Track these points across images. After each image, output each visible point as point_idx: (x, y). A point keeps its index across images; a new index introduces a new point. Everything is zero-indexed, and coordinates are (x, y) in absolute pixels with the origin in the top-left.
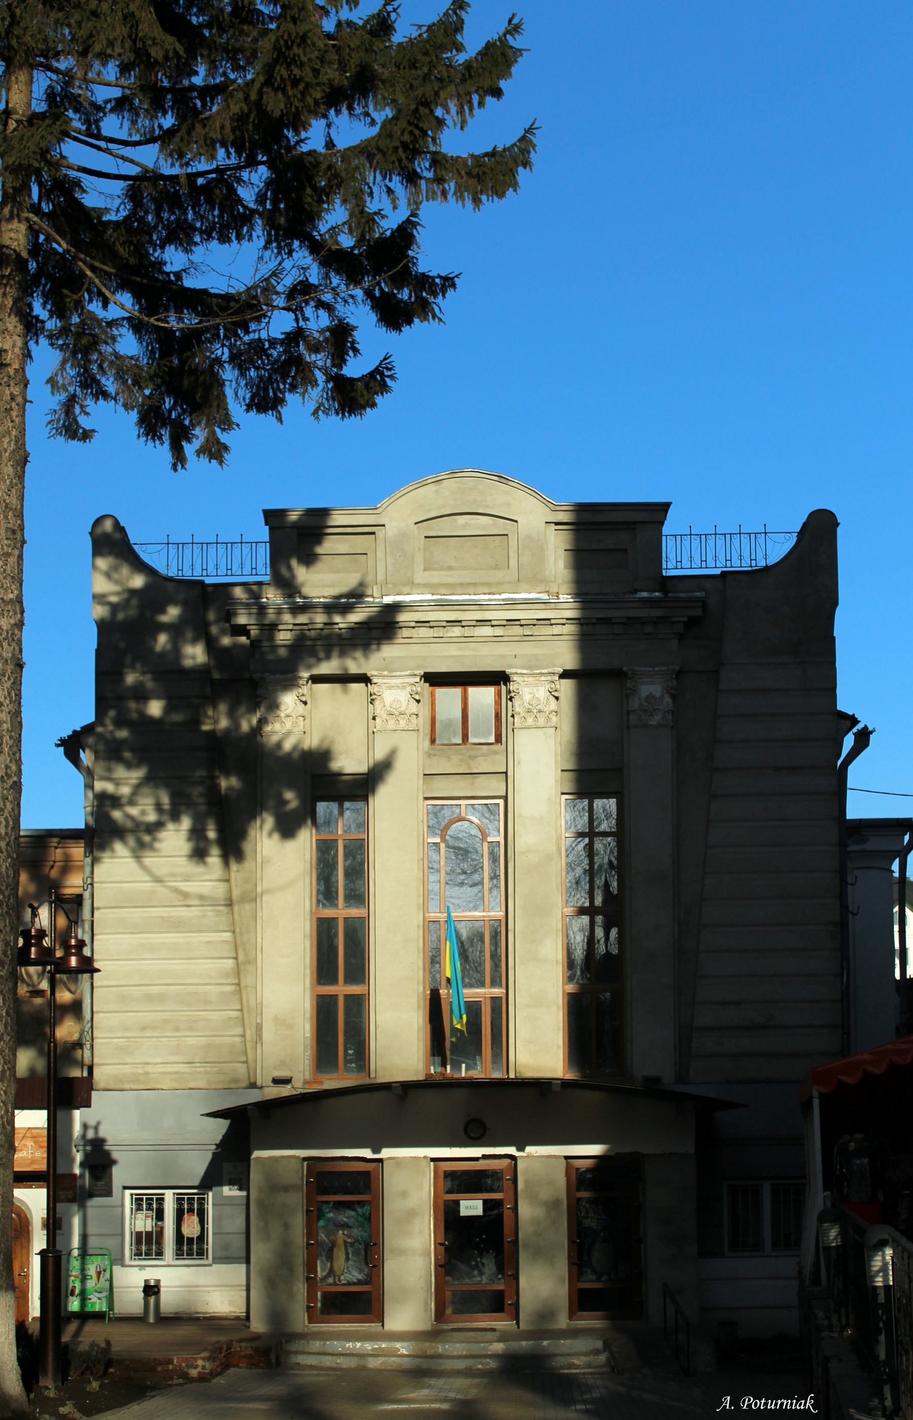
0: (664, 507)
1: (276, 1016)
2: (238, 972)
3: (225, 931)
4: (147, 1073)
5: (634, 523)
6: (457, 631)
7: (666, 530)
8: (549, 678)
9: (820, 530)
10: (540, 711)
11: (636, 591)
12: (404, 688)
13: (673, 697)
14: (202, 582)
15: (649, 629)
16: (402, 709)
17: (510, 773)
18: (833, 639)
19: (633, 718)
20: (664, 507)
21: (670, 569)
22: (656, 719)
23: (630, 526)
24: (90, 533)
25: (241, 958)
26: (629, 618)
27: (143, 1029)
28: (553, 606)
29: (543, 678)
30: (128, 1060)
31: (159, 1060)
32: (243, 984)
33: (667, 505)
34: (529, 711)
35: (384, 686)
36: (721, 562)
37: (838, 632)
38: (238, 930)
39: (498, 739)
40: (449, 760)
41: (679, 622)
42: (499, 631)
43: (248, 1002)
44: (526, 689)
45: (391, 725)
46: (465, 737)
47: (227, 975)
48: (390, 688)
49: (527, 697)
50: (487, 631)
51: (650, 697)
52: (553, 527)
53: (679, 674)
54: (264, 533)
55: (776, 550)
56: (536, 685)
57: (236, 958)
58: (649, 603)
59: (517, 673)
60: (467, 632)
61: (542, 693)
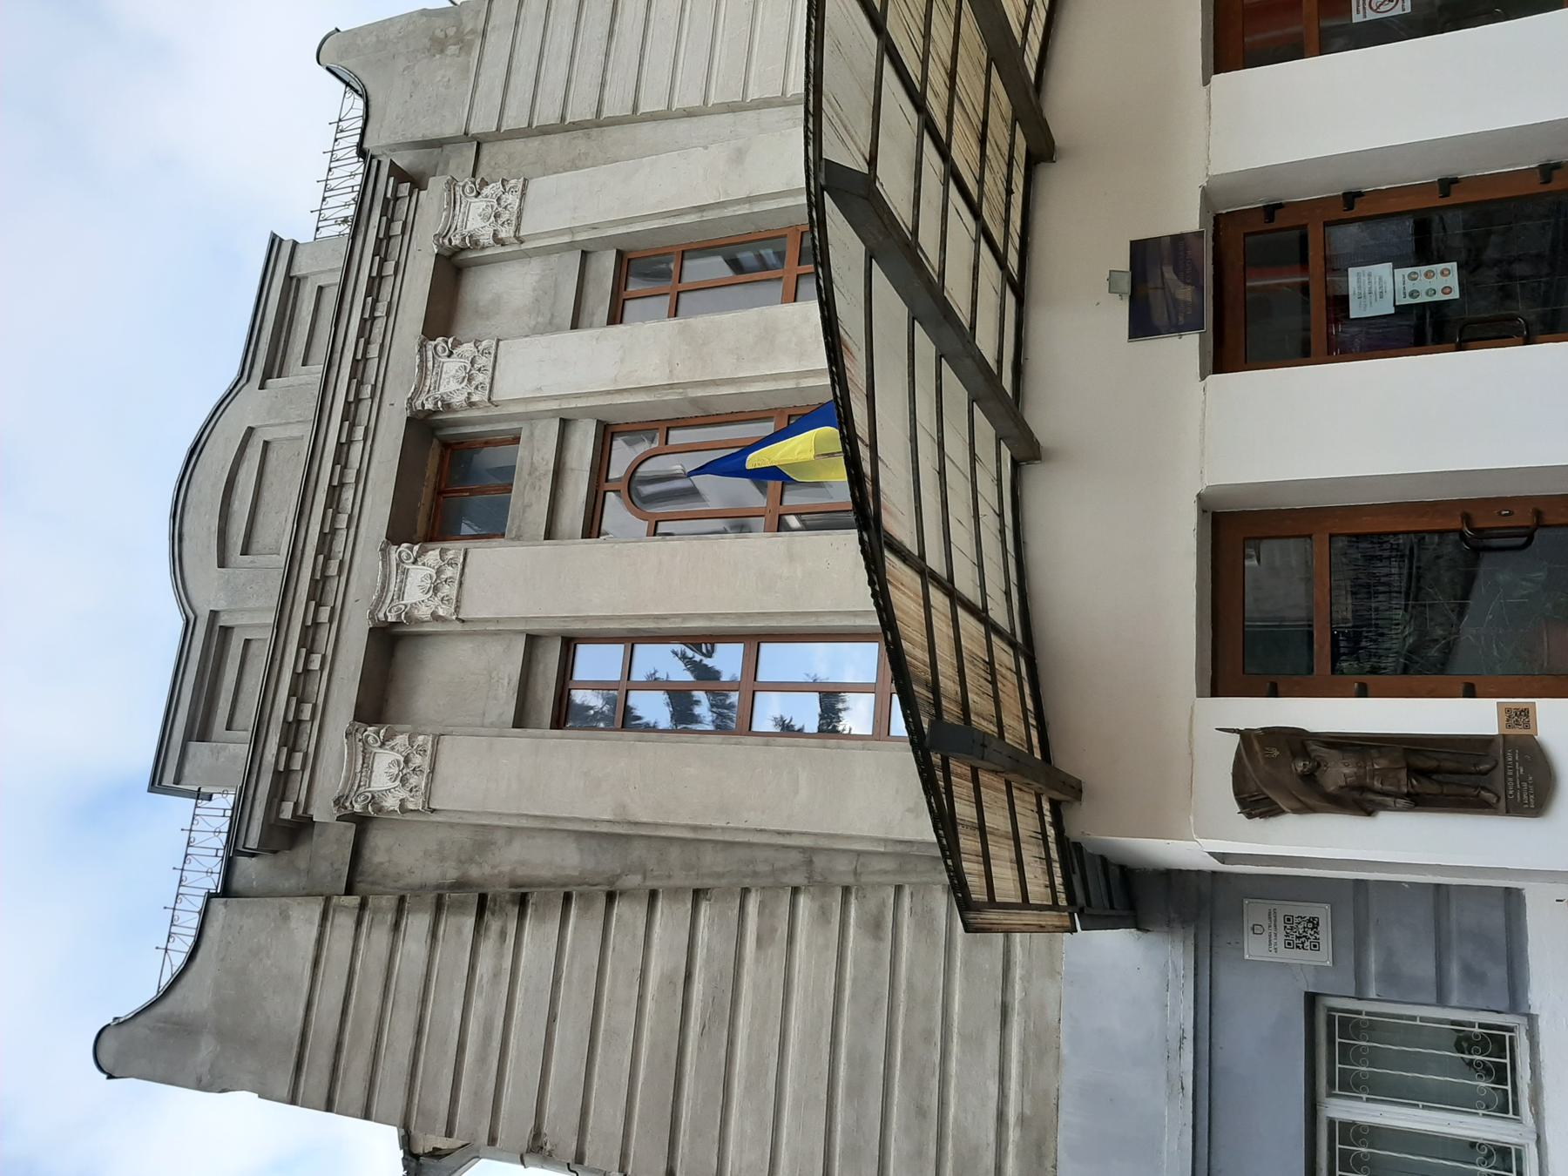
1: (909, 810)
2: (821, 886)
3: (742, 907)
4: (1022, 1120)
5: (289, 278)
6: (348, 494)
8: (430, 354)
10: (473, 363)
12: (406, 572)
14: (210, 896)
15: (397, 228)
16: (433, 572)
17: (554, 405)
19: (506, 233)
22: (512, 199)
24: (110, 1077)
25: (798, 879)
27: (921, 1112)
28: (337, 356)
29: (430, 364)
30: (989, 1160)
31: (993, 1088)
32: (849, 880)
33: (274, 238)
35: (396, 602)
38: (747, 882)
40: (530, 506)
41: (395, 190)
42: (359, 433)
43: (886, 872)
44: (442, 390)
45: (449, 590)
47: (823, 915)
48: (401, 594)
49: (454, 386)
50: (356, 450)
56: (439, 375)
57: (795, 891)
59: (411, 399)
60: (351, 477)
61: (452, 367)
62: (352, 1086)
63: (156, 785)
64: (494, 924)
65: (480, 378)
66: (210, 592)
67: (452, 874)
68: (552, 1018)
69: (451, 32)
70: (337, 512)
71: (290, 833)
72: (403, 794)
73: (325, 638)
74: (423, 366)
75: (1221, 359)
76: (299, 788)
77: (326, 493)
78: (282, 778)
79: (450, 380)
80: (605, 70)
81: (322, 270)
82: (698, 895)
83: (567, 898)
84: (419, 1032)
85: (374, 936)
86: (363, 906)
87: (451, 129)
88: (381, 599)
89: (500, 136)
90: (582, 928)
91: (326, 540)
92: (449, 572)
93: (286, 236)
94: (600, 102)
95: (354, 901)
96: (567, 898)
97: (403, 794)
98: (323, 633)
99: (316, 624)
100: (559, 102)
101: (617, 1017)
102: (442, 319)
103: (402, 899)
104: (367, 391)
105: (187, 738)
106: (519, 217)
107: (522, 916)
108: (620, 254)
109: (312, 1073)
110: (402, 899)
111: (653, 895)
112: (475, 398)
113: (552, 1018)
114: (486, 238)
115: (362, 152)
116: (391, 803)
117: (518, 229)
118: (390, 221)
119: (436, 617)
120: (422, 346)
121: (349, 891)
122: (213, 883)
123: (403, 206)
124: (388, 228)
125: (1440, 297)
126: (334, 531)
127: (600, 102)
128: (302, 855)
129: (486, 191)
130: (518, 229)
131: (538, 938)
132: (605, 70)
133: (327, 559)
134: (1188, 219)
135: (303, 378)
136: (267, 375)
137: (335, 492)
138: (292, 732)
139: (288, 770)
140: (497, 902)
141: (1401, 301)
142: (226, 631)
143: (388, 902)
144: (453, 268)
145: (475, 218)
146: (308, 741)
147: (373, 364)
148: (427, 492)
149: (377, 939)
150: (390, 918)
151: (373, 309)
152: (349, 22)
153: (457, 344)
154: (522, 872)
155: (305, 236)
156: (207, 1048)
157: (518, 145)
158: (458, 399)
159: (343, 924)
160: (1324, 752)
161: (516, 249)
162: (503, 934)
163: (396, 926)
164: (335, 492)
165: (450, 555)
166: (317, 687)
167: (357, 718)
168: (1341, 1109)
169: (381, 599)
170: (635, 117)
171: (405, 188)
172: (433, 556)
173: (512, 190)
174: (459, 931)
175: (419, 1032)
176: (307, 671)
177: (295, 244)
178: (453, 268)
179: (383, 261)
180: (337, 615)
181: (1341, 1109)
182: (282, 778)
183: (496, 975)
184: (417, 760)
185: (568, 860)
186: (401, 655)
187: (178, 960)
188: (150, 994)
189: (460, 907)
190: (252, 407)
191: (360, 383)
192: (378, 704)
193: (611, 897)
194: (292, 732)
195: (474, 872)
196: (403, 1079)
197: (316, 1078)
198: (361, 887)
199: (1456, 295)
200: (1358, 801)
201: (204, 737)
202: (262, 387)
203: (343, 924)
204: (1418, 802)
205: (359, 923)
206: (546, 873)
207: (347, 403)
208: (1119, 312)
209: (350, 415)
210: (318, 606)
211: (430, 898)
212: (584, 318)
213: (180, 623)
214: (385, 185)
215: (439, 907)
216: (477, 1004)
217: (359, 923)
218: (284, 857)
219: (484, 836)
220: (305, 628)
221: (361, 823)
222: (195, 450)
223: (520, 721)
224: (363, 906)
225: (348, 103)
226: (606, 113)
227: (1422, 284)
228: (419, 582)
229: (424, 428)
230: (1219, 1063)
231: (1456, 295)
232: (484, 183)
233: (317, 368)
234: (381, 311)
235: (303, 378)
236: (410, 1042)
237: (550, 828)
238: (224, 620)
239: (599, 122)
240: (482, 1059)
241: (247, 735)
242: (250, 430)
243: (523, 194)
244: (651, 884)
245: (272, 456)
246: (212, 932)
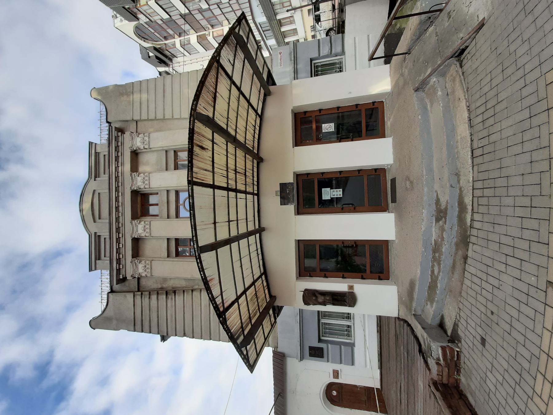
0: (91, 144)
5: (96, 153)
6: (120, 208)
14: (109, 293)
15: (120, 144)
20: (91, 144)
22: (146, 138)
26: (115, 151)
41: (117, 134)
42: (120, 194)
45: (148, 230)
46: (157, 205)
48: (137, 231)
50: (120, 198)
54: (98, 271)
60: (120, 204)
62: (146, 327)
63: (91, 270)
64: (170, 297)
65: (146, 182)
66: (94, 228)
67: (160, 286)
68: (184, 313)
69: (124, 91)
70: (119, 212)
71: (122, 280)
72: (146, 273)
73: (122, 240)
74: (132, 179)
75: (299, 212)
76: (123, 272)
77: (116, 208)
78: (119, 271)
79: (139, 183)
80: (164, 106)
81: (103, 150)
83: (184, 291)
84: (158, 317)
85: (145, 299)
86: (142, 294)
87: (129, 118)
88: (133, 233)
89: (141, 120)
90: (188, 296)
91: (117, 219)
92: (147, 226)
94: (164, 114)
95: (140, 293)
96: (184, 291)
97: (146, 273)
98: (121, 239)
99: (119, 238)
100: (154, 113)
101: (197, 313)
102: (135, 168)
103: (150, 293)
104: (120, 184)
105: (96, 260)
106: (149, 143)
107: (175, 295)
108: (175, 151)
109: (138, 325)
110: (150, 293)
113: (184, 313)
114: (142, 148)
115: (107, 122)
116: (143, 275)
117: (149, 146)
118: (118, 142)
120: (131, 175)
121: (139, 291)
122: (108, 289)
123: (120, 138)
124: (117, 144)
125: (339, 196)
126: (119, 217)
127: (164, 114)
128: (127, 283)
129: (140, 136)
130: (149, 146)
131: (179, 298)
132: (164, 106)
133: (119, 223)
134: (290, 179)
135: (104, 178)
136: (96, 177)
137: (117, 208)
138: (119, 261)
139: (120, 269)
140: (170, 292)
141: (332, 197)
142: (99, 236)
143: (147, 293)
144: (135, 154)
145: (138, 143)
146: (123, 262)
147: (120, 178)
148: (139, 206)
149: (146, 301)
150: (148, 296)
151: (118, 164)
153: (140, 174)
154: (174, 286)
155: (98, 142)
156: (114, 322)
157: (146, 123)
158: (142, 187)
159: (138, 298)
160: (319, 296)
161: (150, 150)
162: (172, 299)
163: (150, 298)
164: (117, 208)
165: (147, 222)
166: (122, 251)
167: (133, 257)
168: (323, 321)
169: (133, 233)
170: (173, 118)
171: (120, 134)
172: (143, 223)
173: (146, 136)
174: (163, 298)
175: (158, 317)
176: (119, 248)
177: (96, 144)
178: (135, 154)
179: (118, 152)
180: (124, 235)
181: (323, 321)
182: (119, 271)
183: (172, 306)
184: (147, 266)
185: (183, 284)
186: (140, 242)
187: (105, 304)
188: (100, 313)
189: (162, 294)
190: (93, 185)
191: (118, 182)
192: (136, 253)
193: (192, 291)
194: (119, 261)
195: (164, 286)
196: (157, 326)
197: (138, 326)
198: (141, 289)
199: (341, 196)
200: (324, 304)
201: (99, 259)
203: (138, 298)
204: (334, 304)
205: (142, 297)
206: (179, 286)
207: (116, 187)
208: (279, 198)
209: (117, 190)
210: (119, 234)
211: (156, 292)
212: (169, 167)
213: (88, 236)
214: (114, 133)
215: (158, 294)
216: (169, 312)
217: (142, 297)
218: (123, 284)
219: (165, 280)
220: (117, 239)
221: (139, 279)
222: (82, 195)
223: (168, 256)
224: (142, 294)
225: (102, 107)
226: (166, 117)
227: (335, 193)
228: (140, 228)
229: (135, 193)
230: (304, 316)
231: (341, 196)
232: (139, 134)
233: (107, 175)
234: (120, 165)
235: (104, 178)
236: (156, 319)
237: (178, 278)
238: (98, 234)
239: (164, 119)
240: (172, 321)
241: (108, 258)
242: (94, 191)
243: (149, 137)
244: (200, 287)
245: (101, 196)
246: (110, 300)
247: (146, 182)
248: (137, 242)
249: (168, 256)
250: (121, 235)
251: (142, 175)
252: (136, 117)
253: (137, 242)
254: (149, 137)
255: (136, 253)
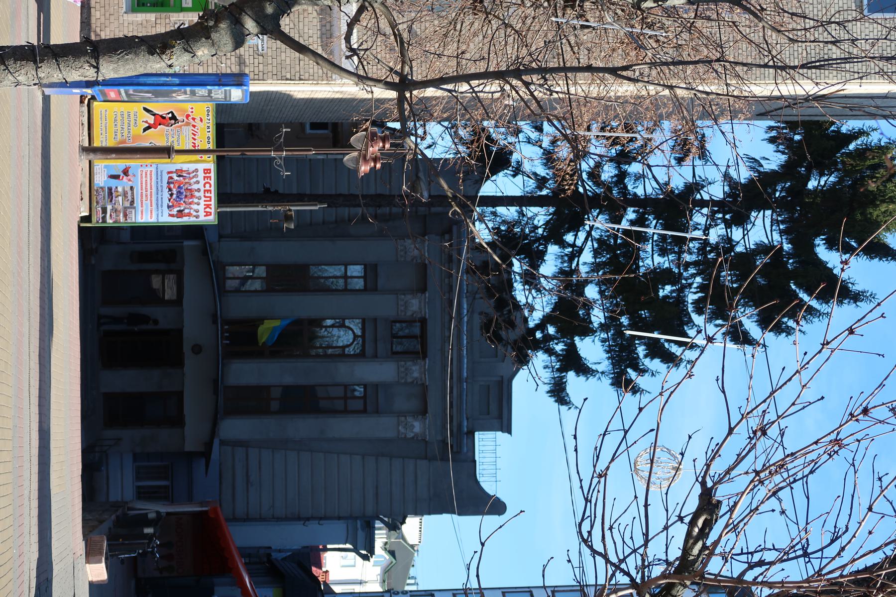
0: (510, 432)
7: (499, 433)
9: (498, 507)
11: (467, 419)
13: (413, 438)
18: (441, 513)
19: (403, 419)
20: (510, 432)
21: (477, 435)
23: (500, 417)
34: (406, 369)
36: (482, 460)
37: (444, 515)
39: (395, 353)
45: (401, 303)
48: (420, 302)
49: (414, 368)
51: (413, 426)
52: (500, 379)
53: (424, 440)
55: (488, 486)
58: (460, 426)
61: (416, 375)
65: (402, 369)
79: (415, 371)
82: (311, 224)
92: (402, 308)
93: (506, 434)
111: (324, 223)
112: (403, 363)
115: (475, 461)
119: (404, 294)
129: (412, 435)
145: (418, 427)
152: (496, 517)
158: (409, 363)
161: (401, 414)
172: (409, 313)
184: (402, 253)
202: (502, 377)
228: (415, 305)
247: (402, 369)
248: (423, 289)
249: (376, 265)
250: (447, 295)
251: (409, 380)
252: (423, 464)
253: (423, 289)
254: (399, 431)
255: (423, 269)
